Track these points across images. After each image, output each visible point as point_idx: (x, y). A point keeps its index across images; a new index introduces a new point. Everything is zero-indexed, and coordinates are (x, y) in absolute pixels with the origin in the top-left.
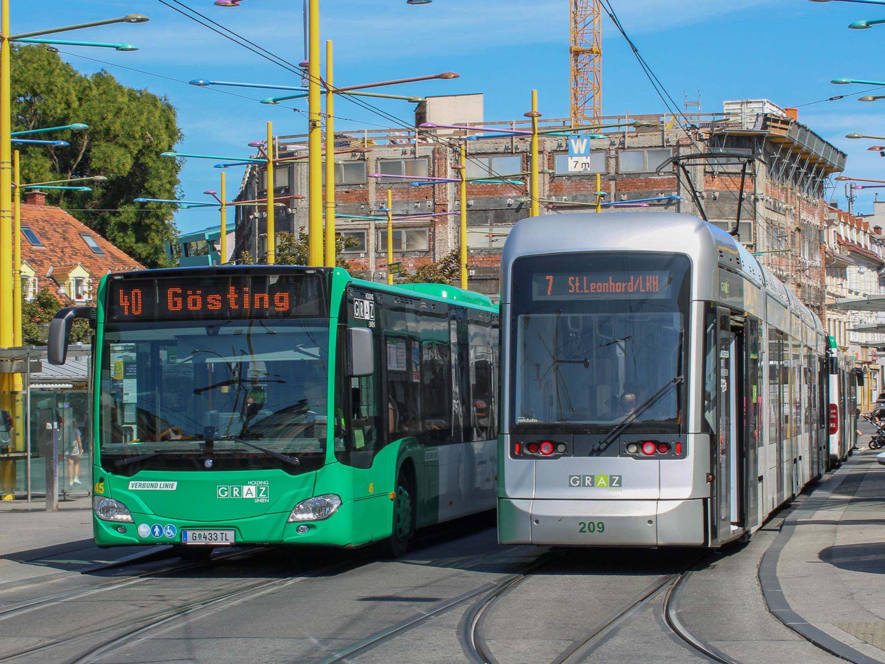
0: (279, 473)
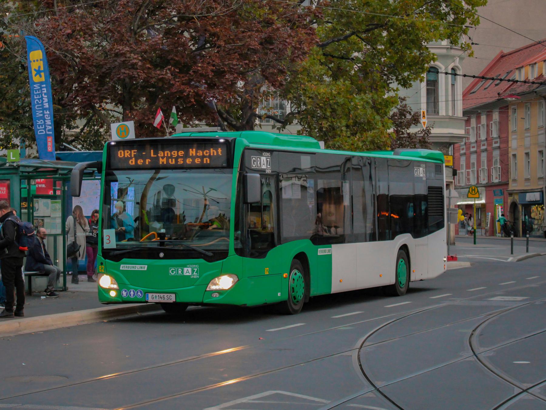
0: (202, 261)
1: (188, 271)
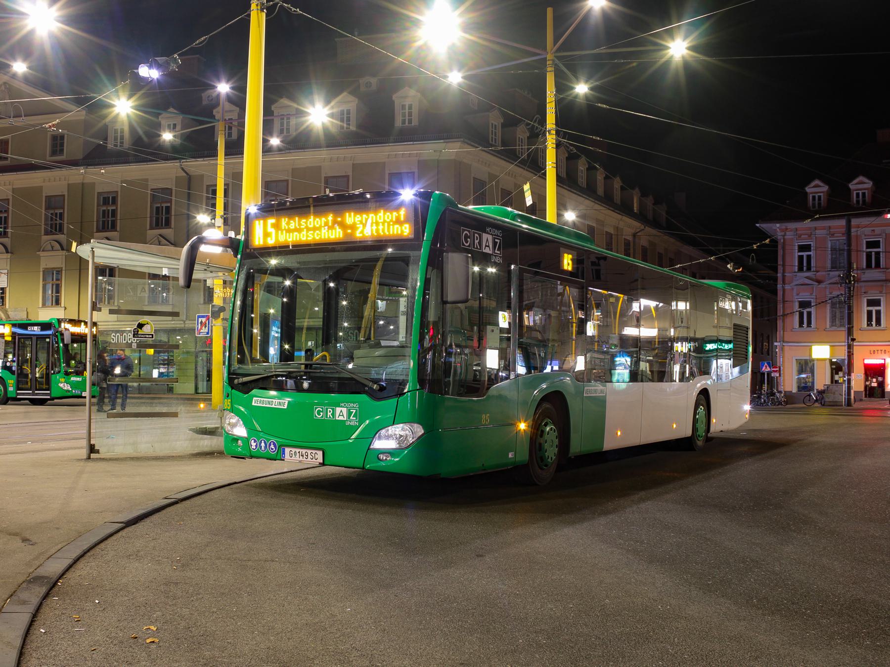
0: (364, 397)
1: (341, 413)
